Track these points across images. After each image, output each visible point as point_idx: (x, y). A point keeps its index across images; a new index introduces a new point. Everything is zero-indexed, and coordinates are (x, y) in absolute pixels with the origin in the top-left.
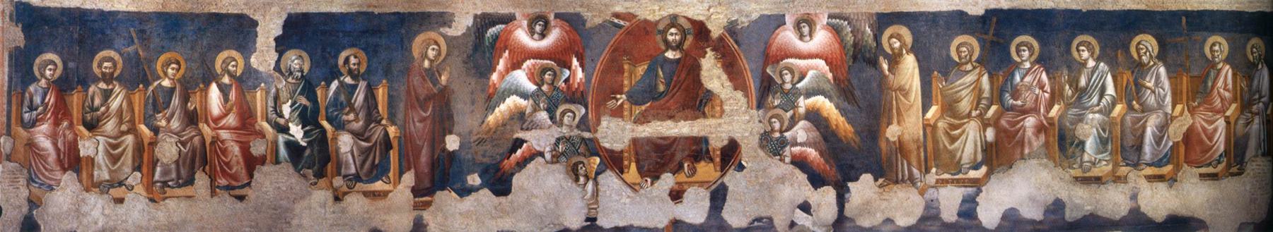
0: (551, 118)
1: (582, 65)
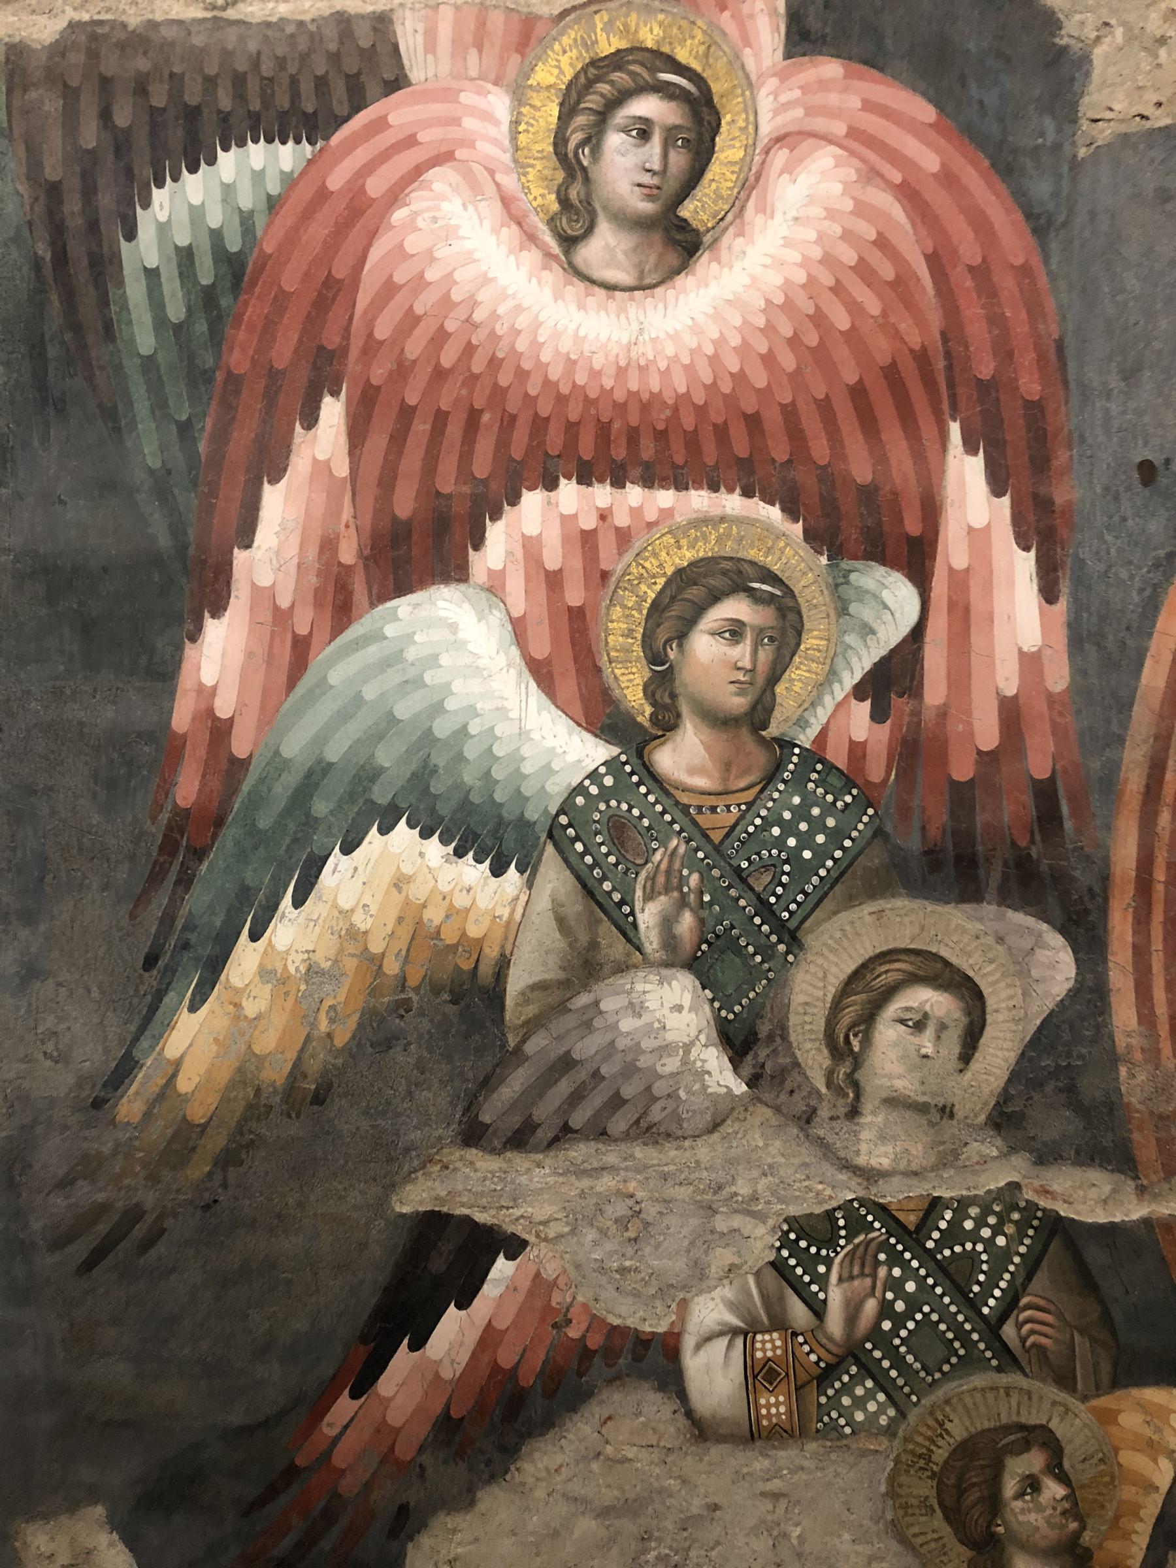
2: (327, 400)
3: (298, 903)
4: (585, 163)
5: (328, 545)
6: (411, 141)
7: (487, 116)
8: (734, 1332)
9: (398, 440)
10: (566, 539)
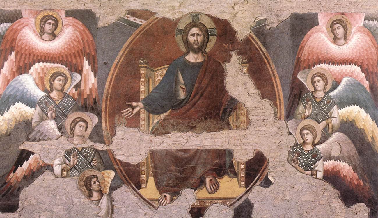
0: (60, 128)
1: (94, 70)
2: (13, 52)
3: (7, 111)
5: (12, 69)
6: (23, 23)
7: (32, 21)
8: (60, 164)
10: (40, 69)
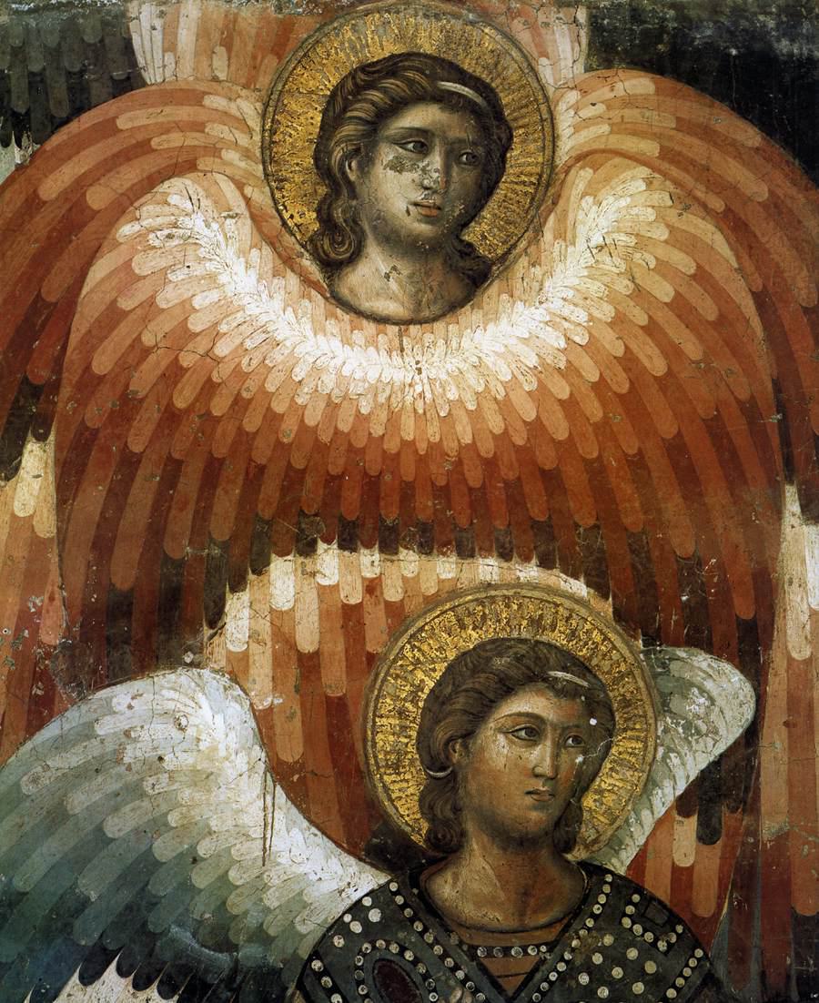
4: (352, 177)
6: (143, 148)
9: (118, 496)
10: (325, 615)
